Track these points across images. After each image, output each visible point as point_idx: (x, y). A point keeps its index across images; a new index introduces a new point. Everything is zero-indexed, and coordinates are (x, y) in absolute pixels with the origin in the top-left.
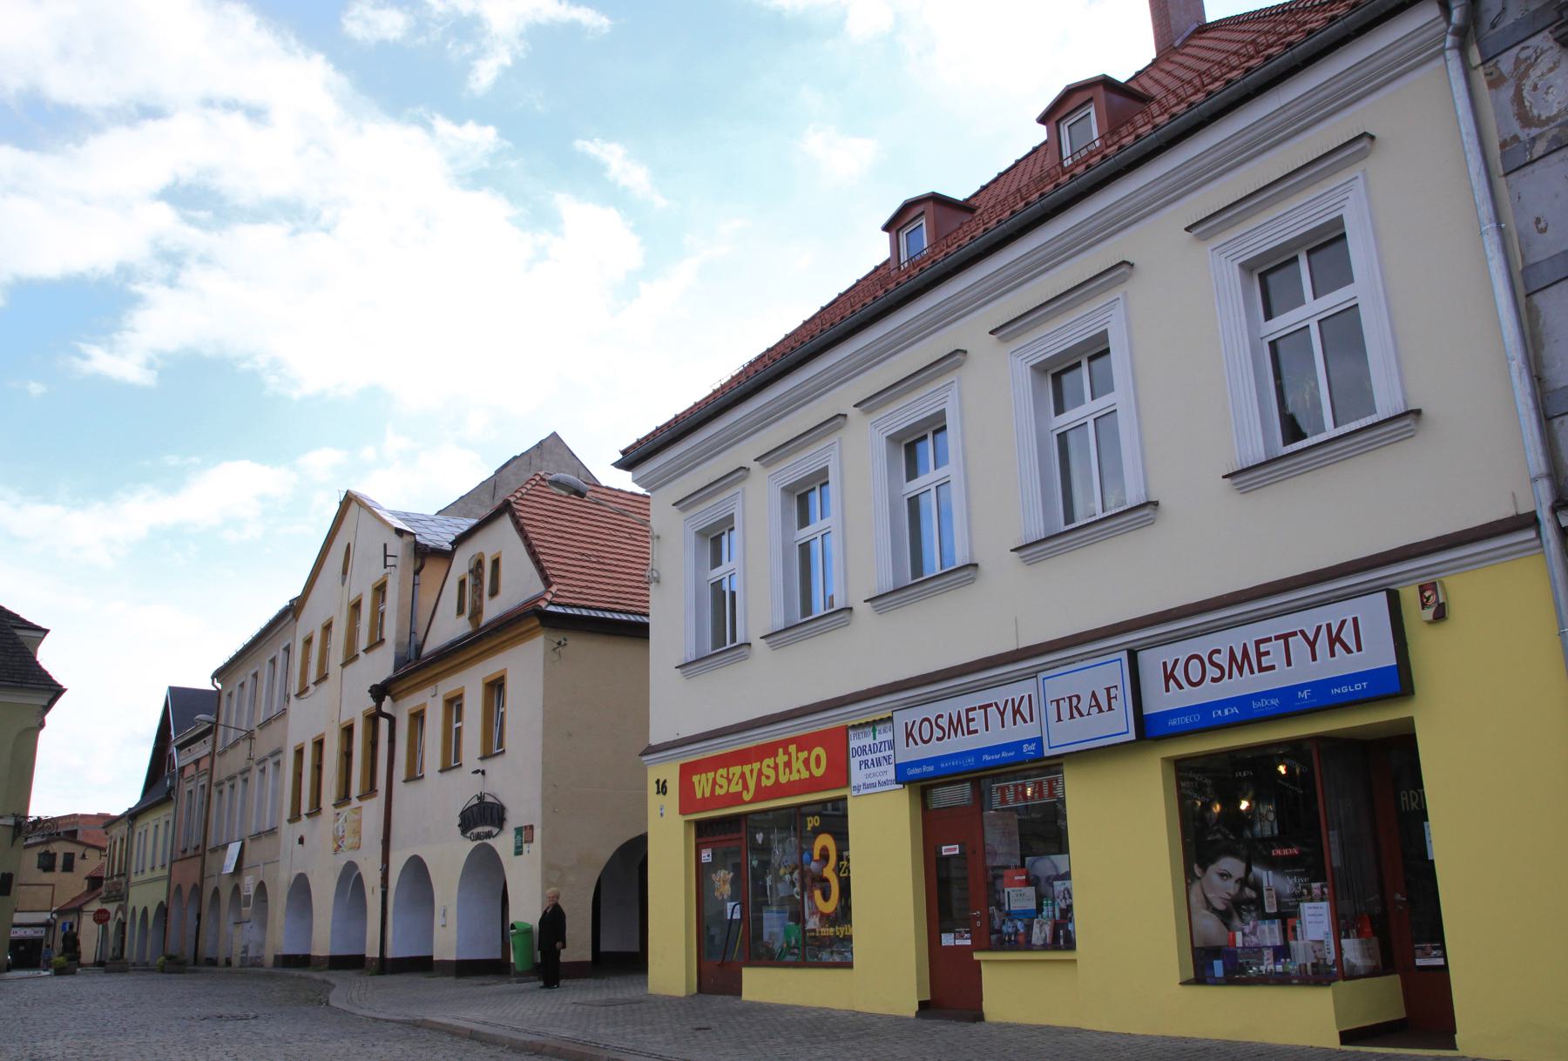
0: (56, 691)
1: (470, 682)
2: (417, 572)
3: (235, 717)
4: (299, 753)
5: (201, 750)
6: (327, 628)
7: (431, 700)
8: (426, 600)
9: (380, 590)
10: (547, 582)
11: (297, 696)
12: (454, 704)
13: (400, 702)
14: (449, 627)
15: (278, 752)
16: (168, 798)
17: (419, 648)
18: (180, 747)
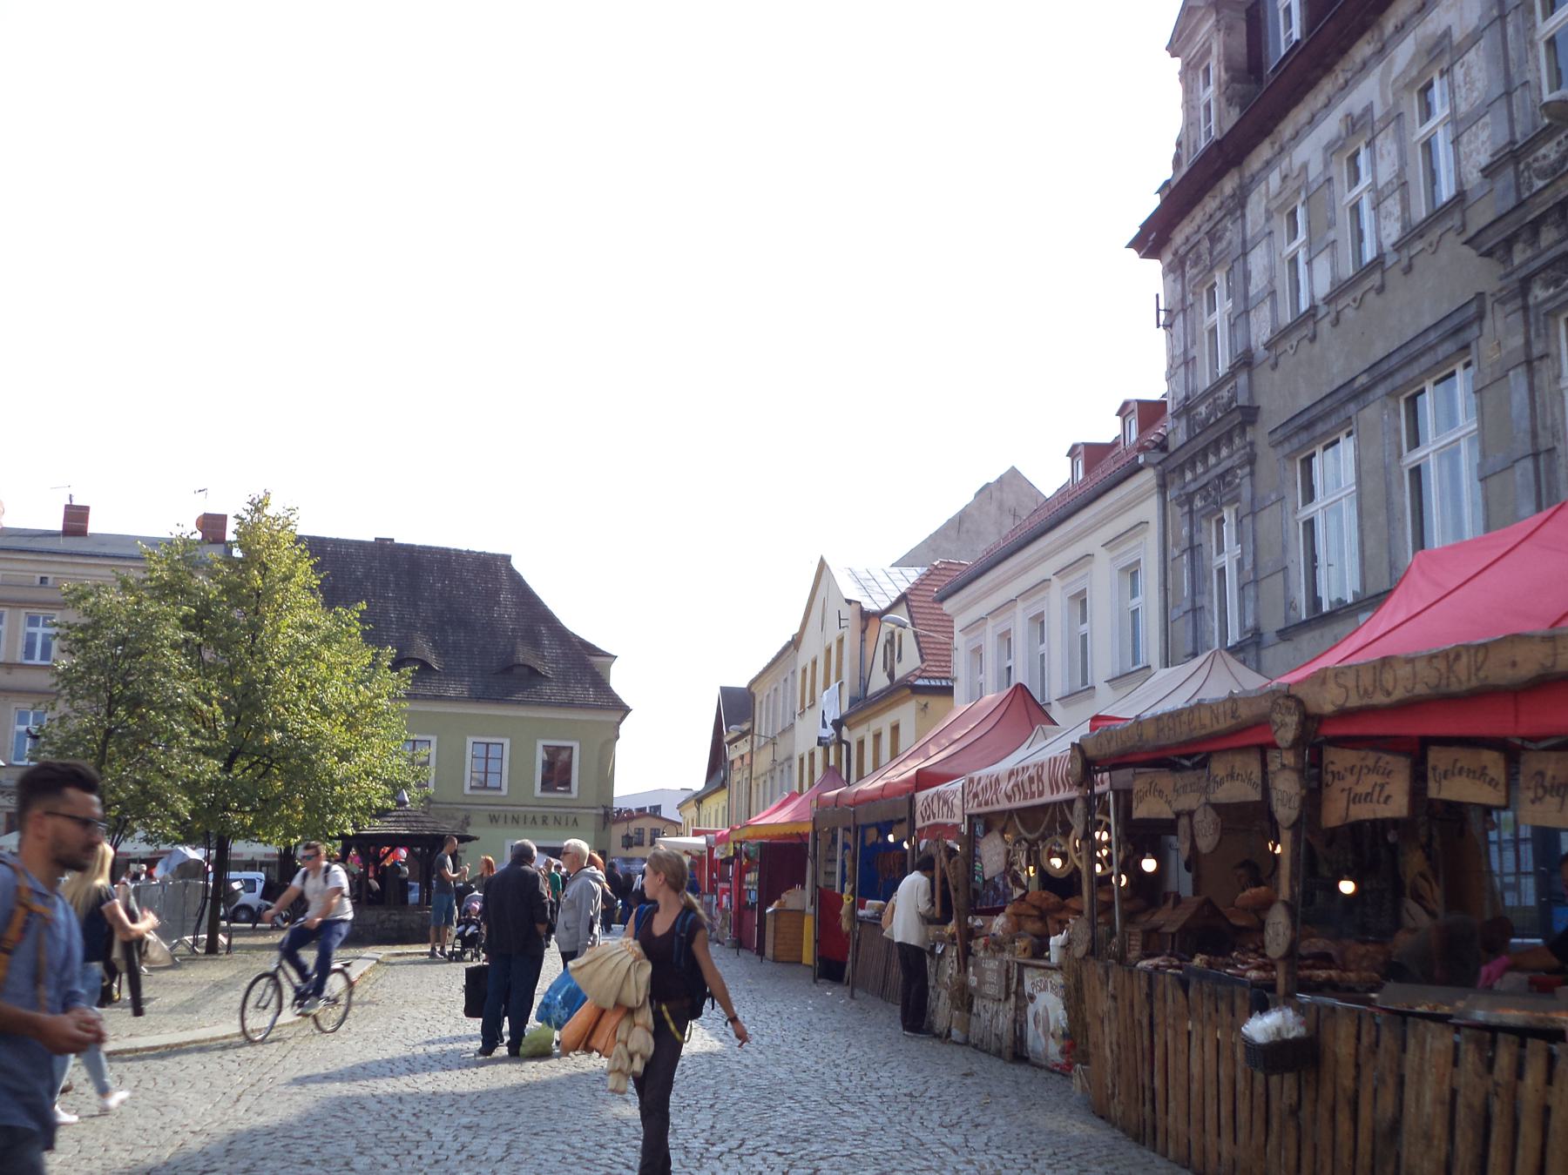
0: (625, 710)
1: (883, 723)
2: (863, 631)
3: (764, 723)
4: (802, 760)
5: (743, 747)
6: (814, 663)
7: (865, 732)
8: (869, 650)
9: (841, 641)
10: (923, 661)
11: (799, 715)
12: (877, 737)
13: (853, 731)
14: (879, 681)
15: (790, 758)
16: (723, 786)
17: (866, 689)
18: (730, 743)
